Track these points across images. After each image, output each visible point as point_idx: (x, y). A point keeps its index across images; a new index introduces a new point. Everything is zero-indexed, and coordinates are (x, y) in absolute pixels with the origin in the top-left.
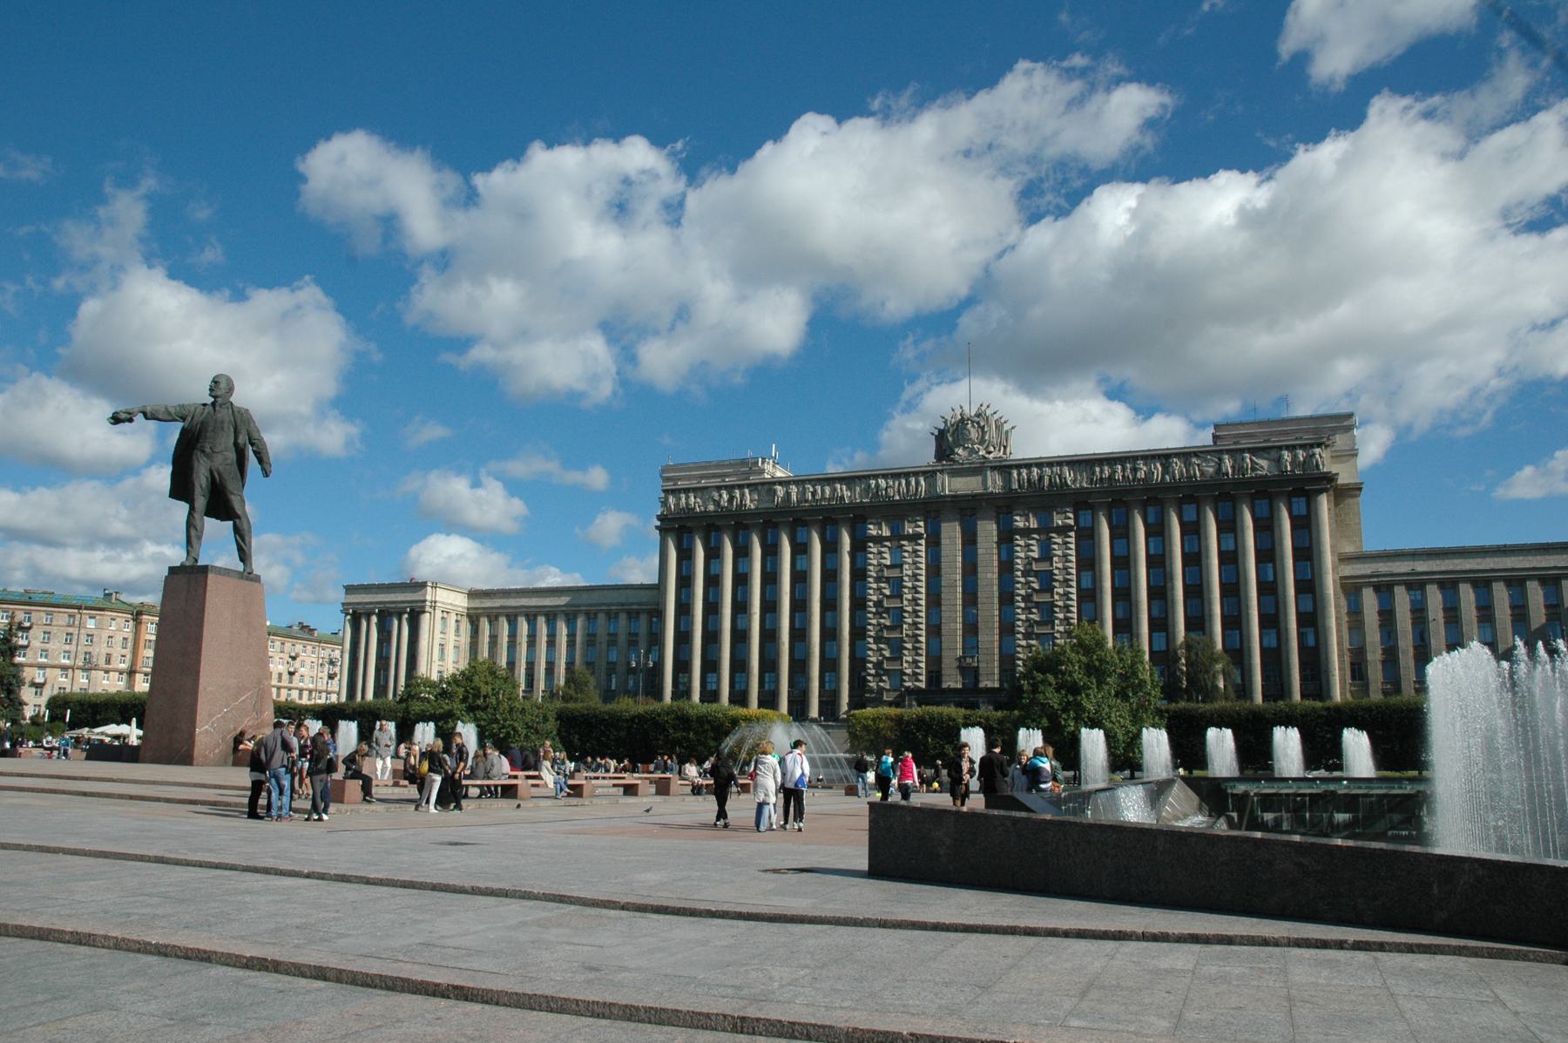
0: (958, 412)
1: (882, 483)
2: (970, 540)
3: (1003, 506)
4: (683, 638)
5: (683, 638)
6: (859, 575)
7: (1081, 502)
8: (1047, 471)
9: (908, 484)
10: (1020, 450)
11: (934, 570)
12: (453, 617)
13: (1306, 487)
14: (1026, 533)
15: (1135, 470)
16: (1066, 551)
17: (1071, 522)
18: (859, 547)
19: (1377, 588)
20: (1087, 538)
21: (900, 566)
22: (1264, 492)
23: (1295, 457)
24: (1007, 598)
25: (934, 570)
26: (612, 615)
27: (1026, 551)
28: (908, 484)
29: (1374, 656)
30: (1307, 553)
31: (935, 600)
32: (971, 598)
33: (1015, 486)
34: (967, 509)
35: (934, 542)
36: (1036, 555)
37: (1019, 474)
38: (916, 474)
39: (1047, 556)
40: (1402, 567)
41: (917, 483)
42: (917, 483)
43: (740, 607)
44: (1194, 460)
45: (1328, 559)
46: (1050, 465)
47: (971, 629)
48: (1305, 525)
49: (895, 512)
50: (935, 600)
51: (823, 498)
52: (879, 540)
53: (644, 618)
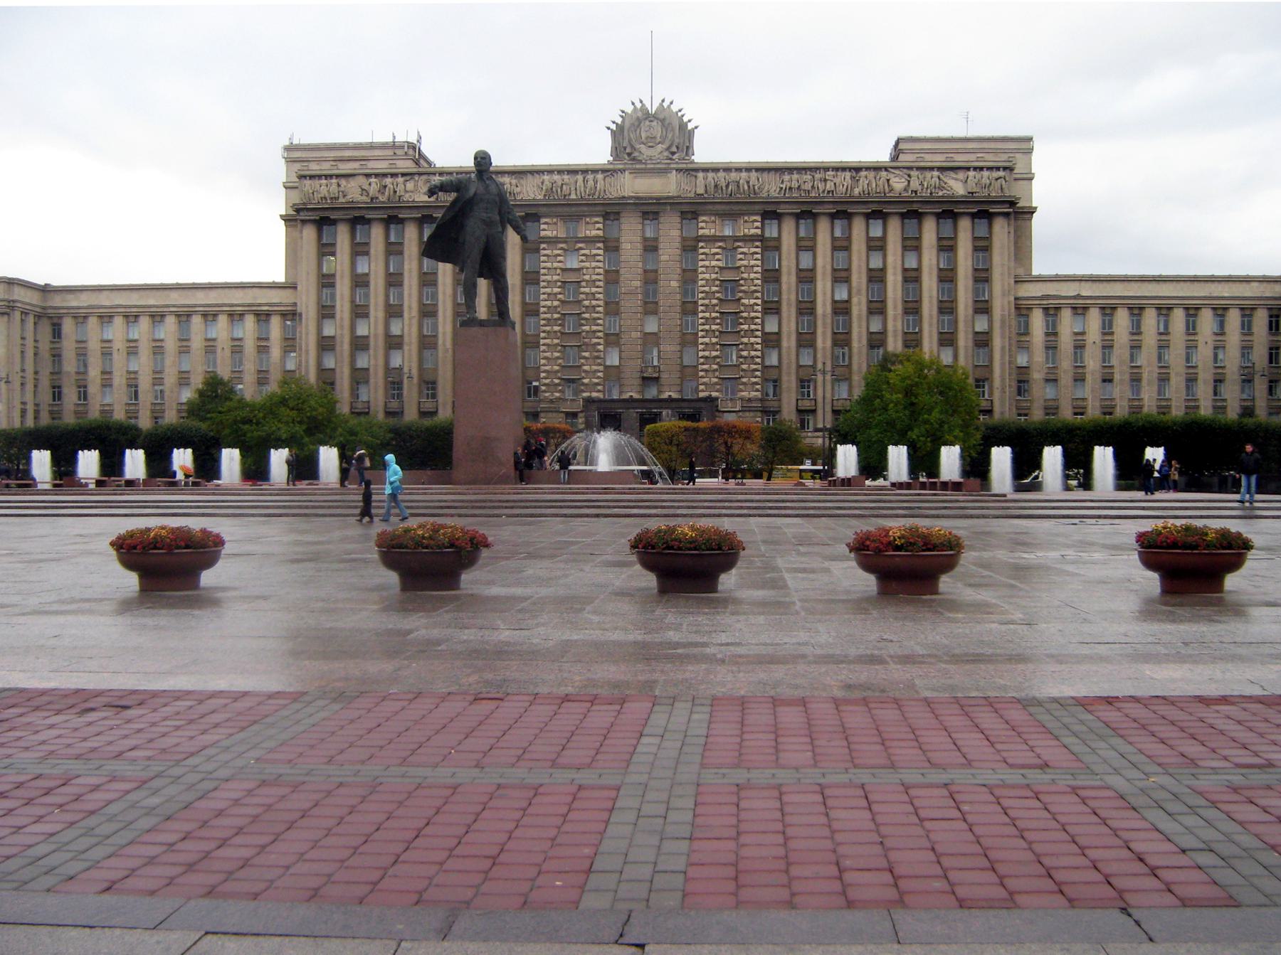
0: (639, 105)
1: (556, 177)
2: (651, 247)
3: (690, 210)
6: (531, 278)
7: (771, 213)
8: (734, 175)
10: (703, 153)
12: (31, 319)
16: (751, 261)
19: (1046, 309)
22: (948, 211)
26: (209, 316)
27: (709, 263)
34: (650, 209)
35: (612, 247)
38: (595, 171)
40: (1069, 290)
41: (596, 182)
42: (596, 182)
46: (739, 170)
48: (982, 247)
49: (571, 210)
53: (275, 322)
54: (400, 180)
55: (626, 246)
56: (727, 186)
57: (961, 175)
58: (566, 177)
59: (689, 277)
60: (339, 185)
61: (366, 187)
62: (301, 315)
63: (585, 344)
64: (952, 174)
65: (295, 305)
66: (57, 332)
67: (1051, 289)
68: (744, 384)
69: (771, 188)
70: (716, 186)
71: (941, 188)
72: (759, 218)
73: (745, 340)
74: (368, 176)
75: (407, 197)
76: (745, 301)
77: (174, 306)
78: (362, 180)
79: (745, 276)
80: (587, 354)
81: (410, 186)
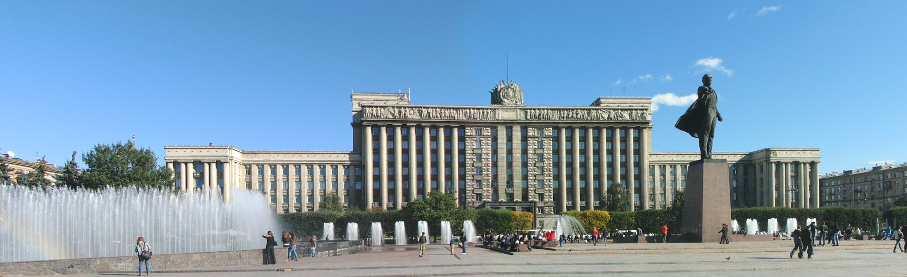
2: (510, 139)
4: (377, 178)
5: (377, 178)
6: (462, 152)
7: (556, 127)
11: (495, 152)
13: (640, 127)
16: (549, 145)
18: (462, 139)
20: (557, 139)
24: (525, 165)
25: (495, 152)
29: (658, 190)
30: (639, 152)
31: (495, 165)
32: (510, 165)
35: (495, 139)
39: (541, 147)
43: (406, 164)
45: (646, 154)
48: (638, 140)
49: (479, 125)
50: (495, 165)
52: (471, 137)
55: (499, 140)
59: (525, 152)
66: (249, 172)
67: (661, 157)
69: (555, 117)
75: (409, 116)
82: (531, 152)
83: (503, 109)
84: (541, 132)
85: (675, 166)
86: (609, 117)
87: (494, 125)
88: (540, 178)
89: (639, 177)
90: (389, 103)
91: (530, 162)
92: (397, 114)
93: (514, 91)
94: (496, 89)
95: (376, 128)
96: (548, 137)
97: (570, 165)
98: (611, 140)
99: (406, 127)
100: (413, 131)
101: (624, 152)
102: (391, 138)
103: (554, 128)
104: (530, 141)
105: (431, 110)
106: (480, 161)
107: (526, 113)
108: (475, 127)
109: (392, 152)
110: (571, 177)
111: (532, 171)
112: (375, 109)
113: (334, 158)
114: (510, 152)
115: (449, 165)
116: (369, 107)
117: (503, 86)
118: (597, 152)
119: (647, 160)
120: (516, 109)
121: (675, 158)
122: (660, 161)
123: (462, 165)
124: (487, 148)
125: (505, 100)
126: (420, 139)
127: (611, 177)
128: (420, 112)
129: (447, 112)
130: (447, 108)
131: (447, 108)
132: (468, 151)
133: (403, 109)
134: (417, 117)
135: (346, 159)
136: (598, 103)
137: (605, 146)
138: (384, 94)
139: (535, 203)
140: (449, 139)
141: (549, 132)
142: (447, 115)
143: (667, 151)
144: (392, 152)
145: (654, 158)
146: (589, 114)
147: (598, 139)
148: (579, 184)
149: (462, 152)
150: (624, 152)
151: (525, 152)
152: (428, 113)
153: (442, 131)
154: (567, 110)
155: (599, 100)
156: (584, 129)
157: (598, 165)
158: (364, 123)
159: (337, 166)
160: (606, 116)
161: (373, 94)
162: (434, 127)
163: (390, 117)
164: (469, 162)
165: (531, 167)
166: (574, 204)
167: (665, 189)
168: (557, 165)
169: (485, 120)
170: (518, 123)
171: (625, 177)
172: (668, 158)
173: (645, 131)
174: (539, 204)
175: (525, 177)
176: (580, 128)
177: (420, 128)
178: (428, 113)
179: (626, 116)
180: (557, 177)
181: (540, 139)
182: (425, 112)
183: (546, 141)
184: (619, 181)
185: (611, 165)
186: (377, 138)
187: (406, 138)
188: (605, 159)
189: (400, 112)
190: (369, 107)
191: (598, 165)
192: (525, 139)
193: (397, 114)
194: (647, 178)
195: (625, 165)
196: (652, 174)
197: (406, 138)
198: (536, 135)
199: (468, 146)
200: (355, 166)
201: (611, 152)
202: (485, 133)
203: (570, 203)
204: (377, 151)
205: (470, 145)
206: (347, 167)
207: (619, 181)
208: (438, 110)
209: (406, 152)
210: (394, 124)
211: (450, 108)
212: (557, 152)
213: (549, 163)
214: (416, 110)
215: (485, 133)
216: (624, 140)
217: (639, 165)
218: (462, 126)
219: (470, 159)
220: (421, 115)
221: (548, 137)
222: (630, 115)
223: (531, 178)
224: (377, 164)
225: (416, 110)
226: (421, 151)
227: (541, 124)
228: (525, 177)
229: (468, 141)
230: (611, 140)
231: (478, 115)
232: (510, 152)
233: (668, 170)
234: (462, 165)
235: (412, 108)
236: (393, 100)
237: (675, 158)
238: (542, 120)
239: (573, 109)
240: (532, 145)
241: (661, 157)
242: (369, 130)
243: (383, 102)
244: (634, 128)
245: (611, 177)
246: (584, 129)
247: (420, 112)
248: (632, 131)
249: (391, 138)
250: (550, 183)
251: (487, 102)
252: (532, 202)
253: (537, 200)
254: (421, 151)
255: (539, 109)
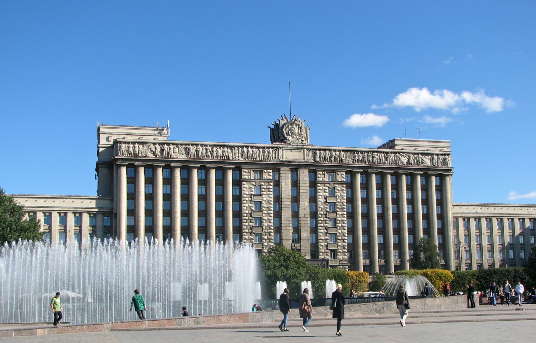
1: (250, 150)
2: (295, 184)
6: (238, 199)
7: (350, 172)
8: (334, 153)
9: (264, 152)
11: (278, 199)
14: (324, 183)
15: (373, 157)
16: (342, 193)
17: (271, 178)
18: (238, 183)
20: (351, 186)
21: (261, 195)
23: (439, 159)
24: (314, 215)
25: (278, 199)
28: (264, 152)
30: (442, 202)
31: (278, 215)
32: (296, 215)
33: (318, 159)
35: (277, 184)
36: (327, 194)
37: (320, 153)
41: (269, 153)
42: (269, 153)
44: (398, 155)
45: (450, 206)
47: (297, 230)
48: (441, 189)
49: (258, 167)
50: (278, 215)
51: (217, 155)
52: (249, 181)
54: (172, 147)
55: (283, 184)
56: (330, 158)
57: (430, 157)
58: (255, 150)
59: (313, 199)
60: (139, 148)
61: (154, 149)
62: (116, 214)
63: (265, 232)
64: (427, 157)
65: (112, 209)
67: (464, 209)
68: (340, 252)
69: (348, 160)
70: (325, 157)
71: (422, 163)
72: (344, 173)
73: (340, 231)
74: (154, 144)
76: (340, 213)
77: (41, 207)
78: (152, 146)
79: (339, 201)
80: (266, 237)
81: (177, 150)
82: (321, 200)
83: (287, 149)
84: (334, 176)
85: (480, 219)
86: (408, 162)
87: (277, 167)
88: (333, 231)
89: (443, 231)
90: (144, 139)
91: (321, 212)
92: (158, 152)
93: (300, 128)
94: (277, 125)
95: (132, 167)
96: (341, 183)
97: (367, 216)
98: (411, 188)
99: (169, 167)
100: (178, 172)
101: (426, 202)
102: (151, 181)
103: (347, 172)
104: (320, 187)
105: (200, 148)
106: (260, 210)
107: (315, 154)
108: (255, 170)
109: (151, 197)
110: (367, 231)
111: (323, 223)
112: (131, 146)
113: (78, 204)
114: (296, 200)
115: (221, 214)
116: (125, 143)
117: (285, 121)
118: (397, 201)
119: (451, 212)
120: (303, 149)
121: (479, 210)
122: (463, 213)
123: (238, 214)
124: (268, 195)
125: (290, 138)
126: (186, 182)
127: (413, 231)
128: (187, 151)
129: (220, 151)
130: (220, 146)
131: (220, 146)
132: (246, 198)
133: (166, 147)
134: (183, 156)
135: (92, 205)
136: (391, 144)
137: (405, 195)
138: (139, 127)
139: (327, 261)
140: (221, 183)
141: (342, 177)
142: (220, 154)
143: (471, 202)
144: (151, 197)
145: (457, 210)
146: (386, 158)
147: (396, 187)
148: (377, 239)
149: (238, 199)
150: (426, 202)
151: (313, 199)
152: (197, 151)
153: (213, 173)
154: (362, 152)
155: (392, 141)
156: (382, 176)
157: (397, 216)
158: (119, 163)
159: (81, 214)
160: (405, 160)
161: (124, 127)
162: (204, 168)
163: (150, 155)
164: (246, 211)
165: (321, 218)
166: (372, 262)
167: (470, 245)
168: (352, 216)
169: (265, 161)
170: (305, 166)
171: (428, 231)
172: (471, 210)
173: (448, 178)
174: (332, 263)
175: (314, 230)
176: (377, 174)
177: (186, 168)
178: (197, 151)
179: (427, 161)
180: (352, 231)
181: (331, 186)
182: (193, 150)
183: (338, 187)
184: (421, 235)
185: (412, 217)
186: (133, 181)
187: (169, 181)
188: (406, 209)
189: (162, 150)
190: (125, 143)
191: (397, 216)
192: (313, 184)
193: (158, 152)
194: (451, 232)
195: (427, 217)
196: (457, 228)
197: (169, 181)
198: (327, 180)
199: (246, 192)
200: (104, 214)
201: (412, 202)
202: (266, 176)
203: (367, 261)
204: (132, 196)
205: (247, 190)
206: (93, 215)
207: (421, 235)
208: (209, 148)
209: (168, 197)
210: (155, 164)
211: (223, 146)
212: (351, 200)
213: (342, 214)
214: (182, 148)
215: (266, 176)
216: (426, 188)
217: (442, 217)
218: (238, 168)
219: (247, 207)
220: (187, 154)
221: (341, 183)
222: (432, 160)
223: (321, 231)
224: (132, 212)
225: (182, 148)
226: (186, 197)
227: (333, 168)
228: (314, 230)
229: (245, 185)
230: (411, 188)
231: (257, 155)
232: (296, 200)
233: (473, 223)
234: (238, 214)
235: (177, 145)
236: (149, 135)
237: (479, 210)
238: (334, 163)
239: (368, 152)
240: (322, 192)
241: (464, 209)
242: (124, 170)
243: (138, 137)
244: (436, 176)
245: (413, 231)
246: (382, 176)
247: (187, 151)
248: (433, 178)
249: (151, 181)
250: (344, 238)
251: (265, 140)
252: (324, 260)
253: (329, 258)
254: (186, 197)
255: (330, 150)
